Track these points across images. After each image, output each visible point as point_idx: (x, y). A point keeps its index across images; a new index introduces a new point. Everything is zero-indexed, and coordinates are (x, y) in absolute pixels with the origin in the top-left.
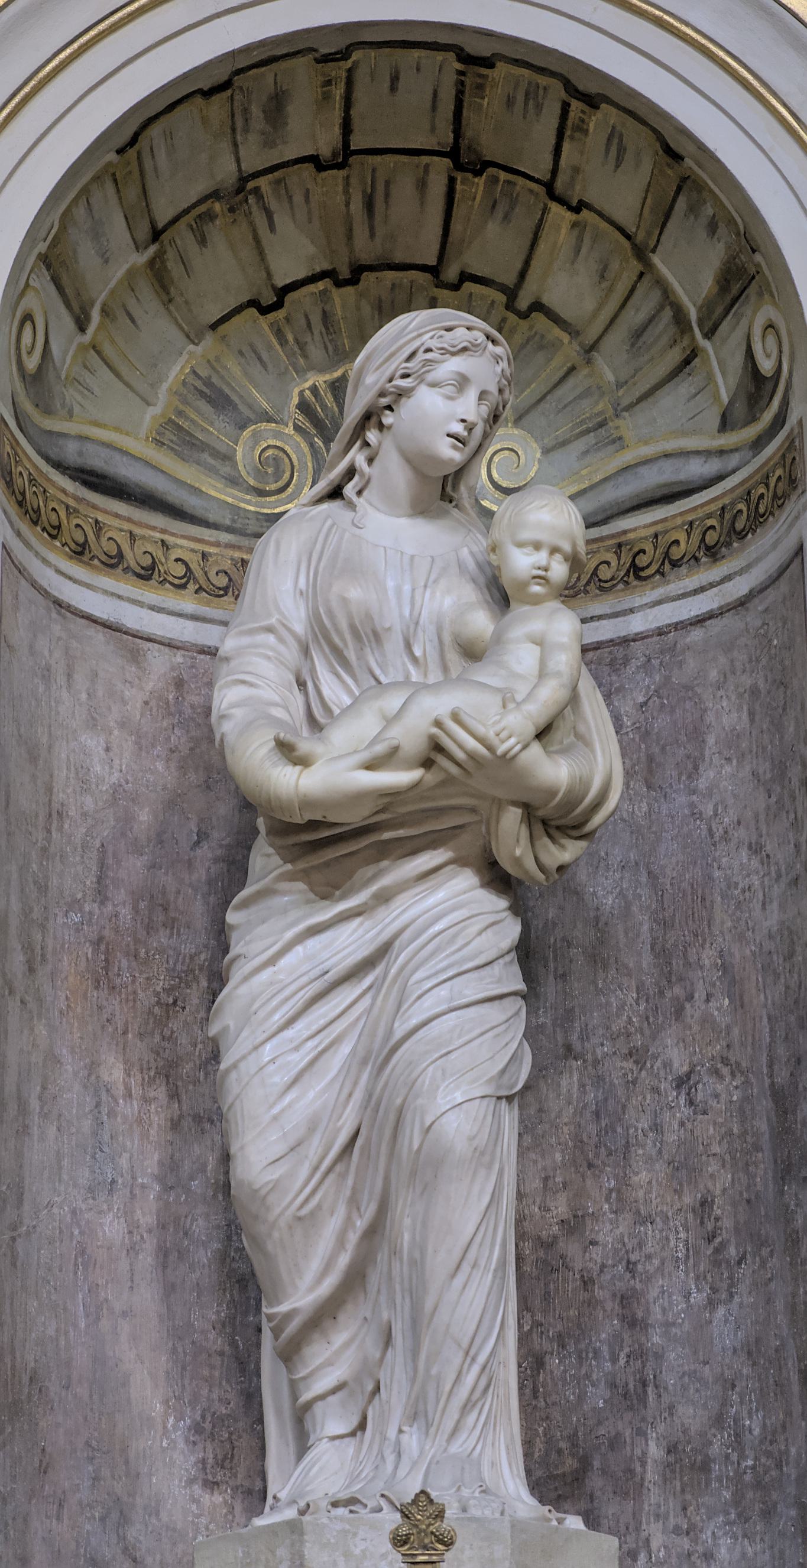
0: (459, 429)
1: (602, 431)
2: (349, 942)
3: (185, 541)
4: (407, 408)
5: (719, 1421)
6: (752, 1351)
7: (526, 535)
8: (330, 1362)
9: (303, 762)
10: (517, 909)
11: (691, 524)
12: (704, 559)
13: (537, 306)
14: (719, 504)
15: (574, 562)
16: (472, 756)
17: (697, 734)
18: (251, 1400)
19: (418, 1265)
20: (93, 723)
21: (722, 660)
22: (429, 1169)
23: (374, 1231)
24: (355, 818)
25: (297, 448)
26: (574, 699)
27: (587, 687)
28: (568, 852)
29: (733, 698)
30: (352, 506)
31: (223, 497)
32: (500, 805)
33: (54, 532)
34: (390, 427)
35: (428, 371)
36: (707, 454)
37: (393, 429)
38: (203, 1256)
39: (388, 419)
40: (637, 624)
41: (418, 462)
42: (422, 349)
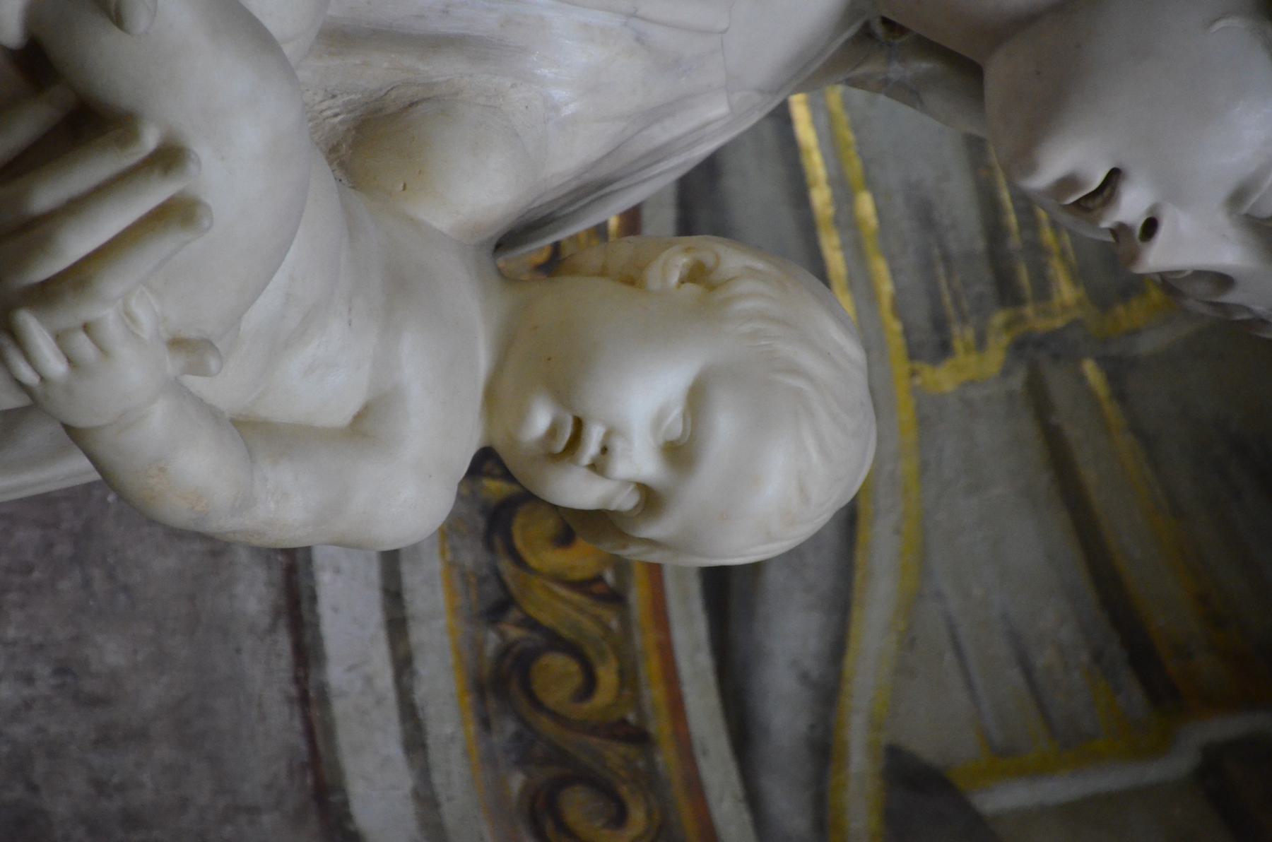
11: (616, 598)
12: (492, 640)
14: (660, 726)
16: (35, 231)
21: (152, 694)
29: (19, 731)
36: (828, 692)
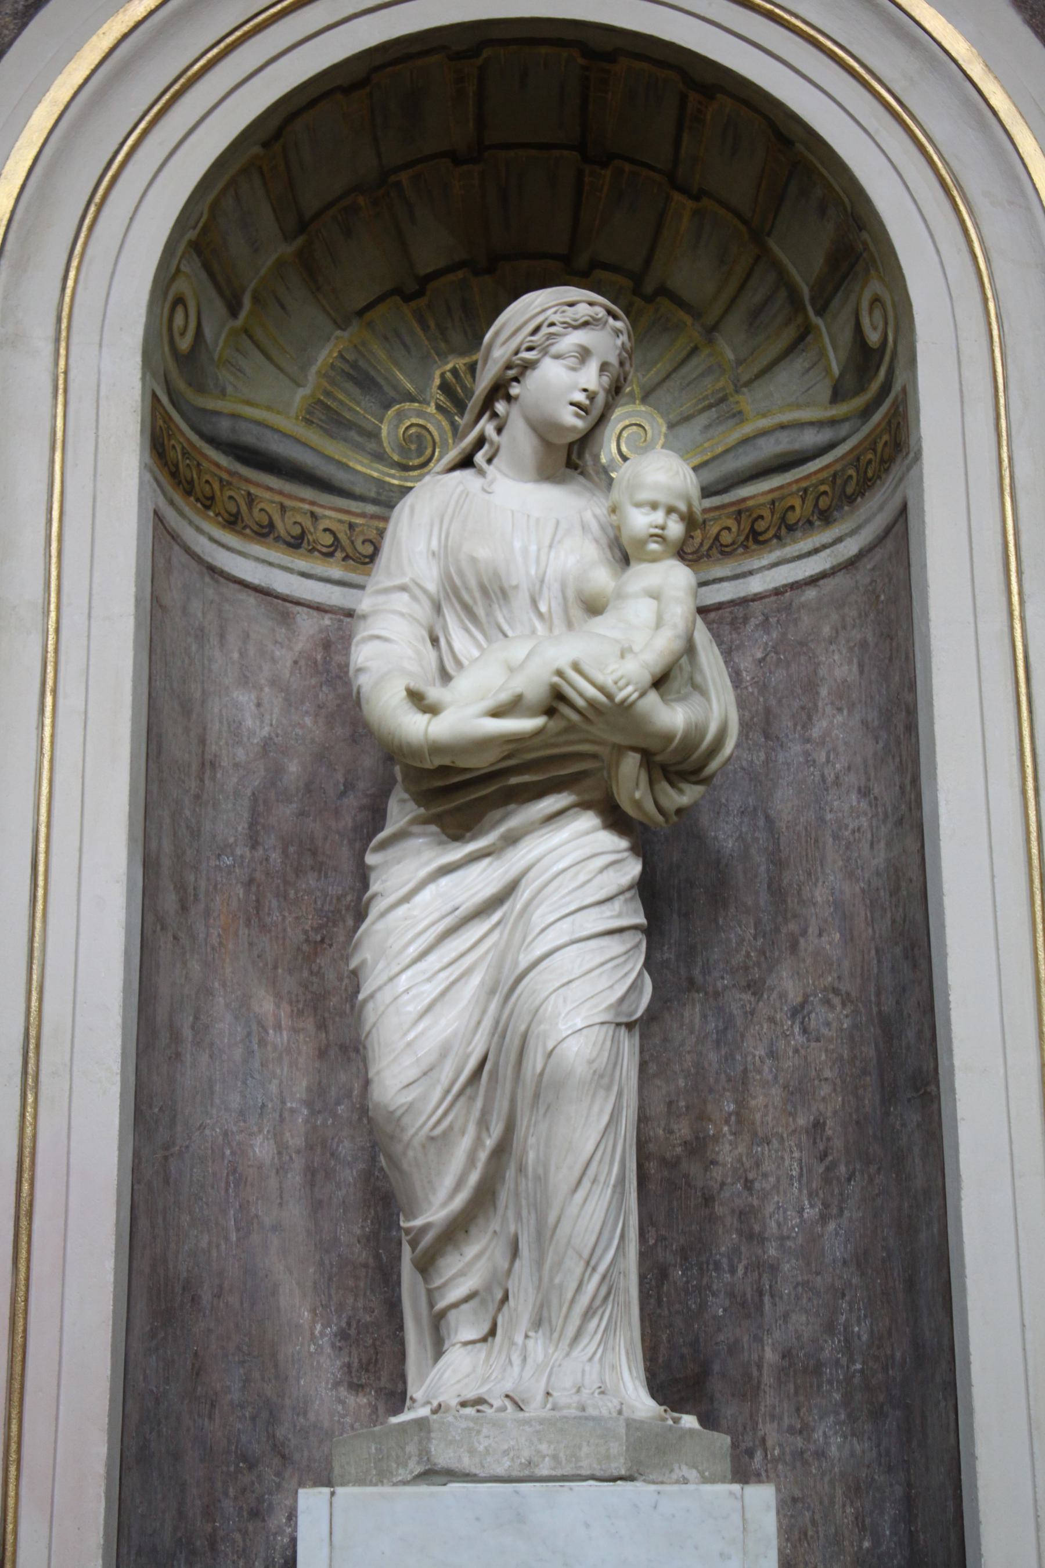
0: (580, 397)
1: (723, 406)
2: (481, 880)
3: (332, 512)
4: (533, 379)
5: (830, 1328)
6: (861, 1260)
7: (644, 496)
8: (465, 1272)
9: (432, 710)
10: (636, 849)
11: (805, 490)
12: (817, 523)
13: (663, 291)
14: (831, 471)
15: (690, 521)
16: (592, 704)
17: (811, 687)
18: (393, 1309)
19: (541, 1180)
20: (245, 680)
21: (835, 617)
22: (547, 1091)
23: (502, 1151)
24: (482, 762)
25: (437, 425)
26: (690, 649)
27: (702, 637)
28: (687, 795)
29: (844, 651)
30: (482, 473)
31: (369, 472)
32: (620, 750)
33: (208, 503)
34: (516, 398)
35: (552, 344)
36: (820, 424)
37: (521, 399)
38: (349, 1175)
39: (515, 390)
40: (756, 585)
41: (544, 431)
42: (546, 324)
